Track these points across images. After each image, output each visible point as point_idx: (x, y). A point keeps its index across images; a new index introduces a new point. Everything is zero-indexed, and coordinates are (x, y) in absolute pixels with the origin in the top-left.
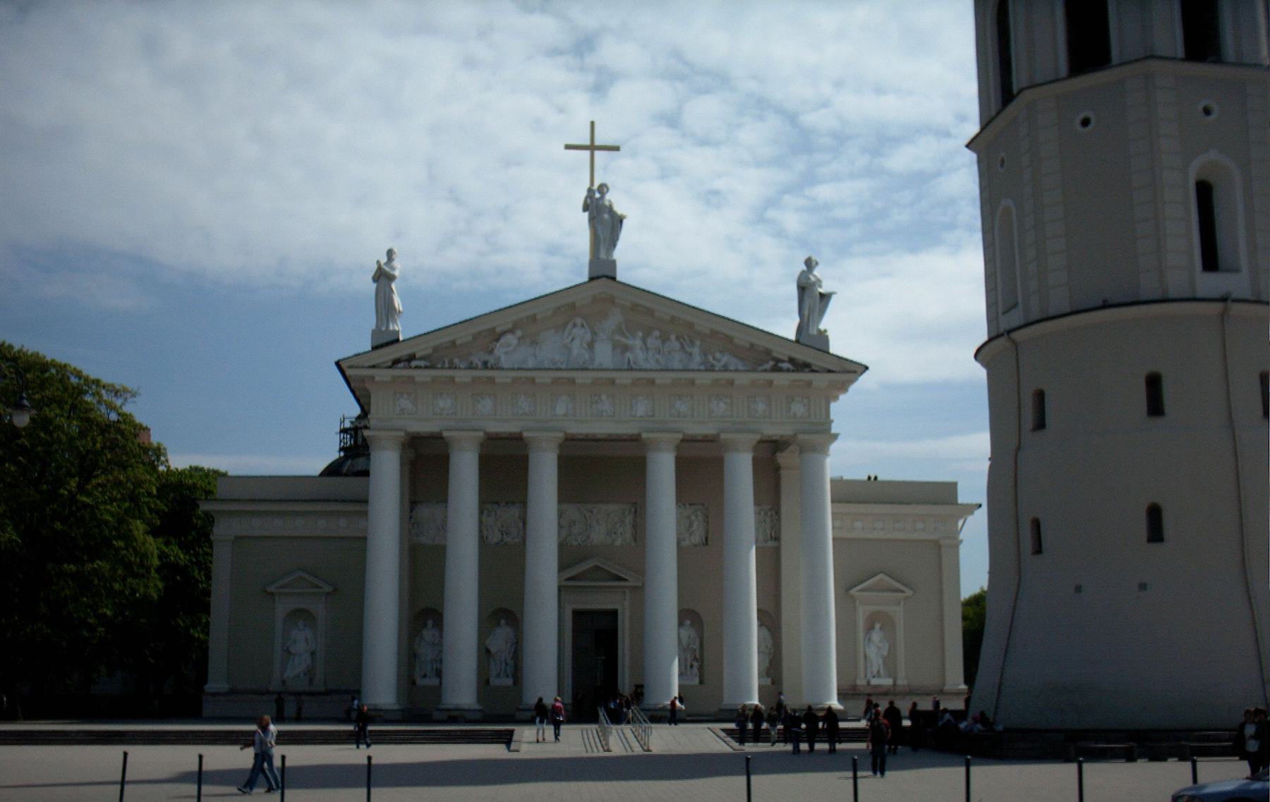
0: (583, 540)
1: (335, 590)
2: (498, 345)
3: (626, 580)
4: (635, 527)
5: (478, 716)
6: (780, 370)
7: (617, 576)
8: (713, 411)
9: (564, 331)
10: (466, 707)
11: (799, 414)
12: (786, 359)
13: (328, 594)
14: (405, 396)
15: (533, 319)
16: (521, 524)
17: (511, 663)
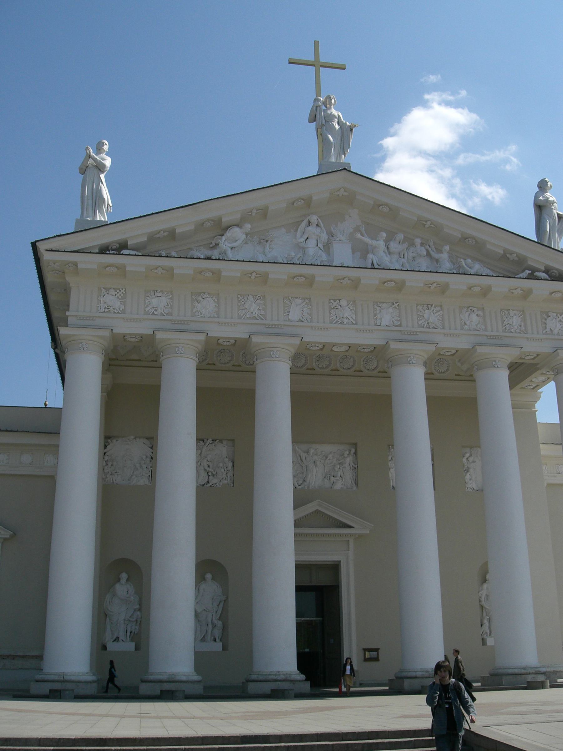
0: (301, 482)
1: (14, 535)
2: (224, 238)
3: (350, 527)
4: (356, 469)
5: (199, 689)
6: (537, 278)
7: (341, 522)
8: (465, 324)
9: (296, 230)
10: (184, 678)
11: (556, 331)
12: (544, 269)
13: (5, 539)
14: (112, 292)
15: (264, 213)
16: (230, 464)
17: (219, 624)
